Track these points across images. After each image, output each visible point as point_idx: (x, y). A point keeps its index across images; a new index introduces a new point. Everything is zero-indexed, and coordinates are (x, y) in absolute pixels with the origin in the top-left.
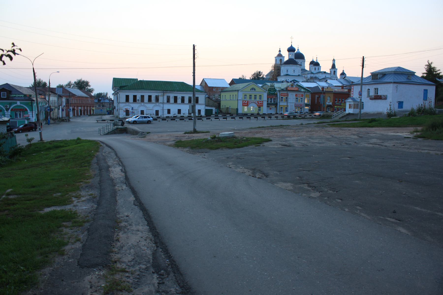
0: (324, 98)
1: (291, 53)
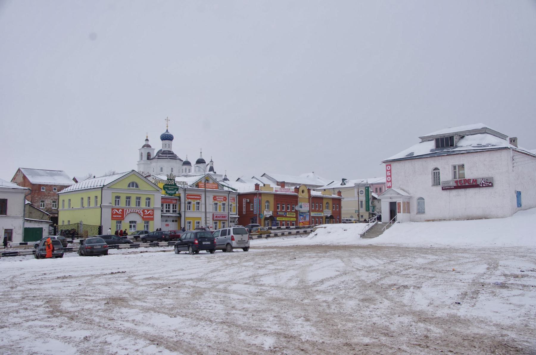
1: (167, 142)
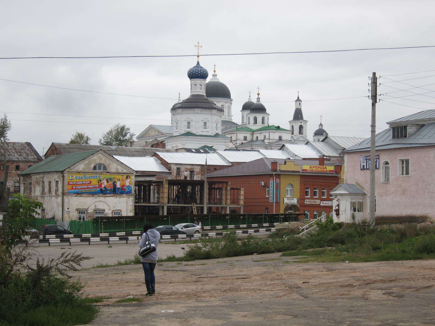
0: (278, 187)
1: (198, 81)
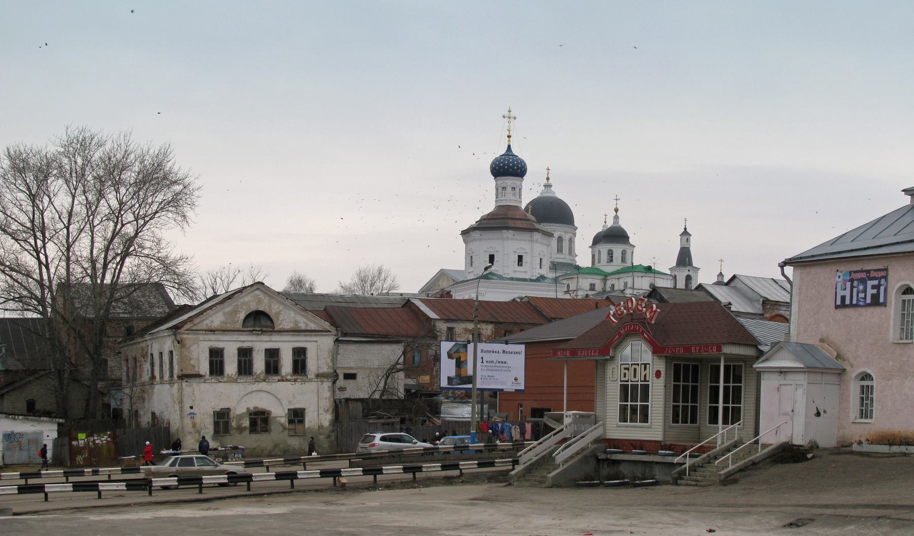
1: (509, 181)
